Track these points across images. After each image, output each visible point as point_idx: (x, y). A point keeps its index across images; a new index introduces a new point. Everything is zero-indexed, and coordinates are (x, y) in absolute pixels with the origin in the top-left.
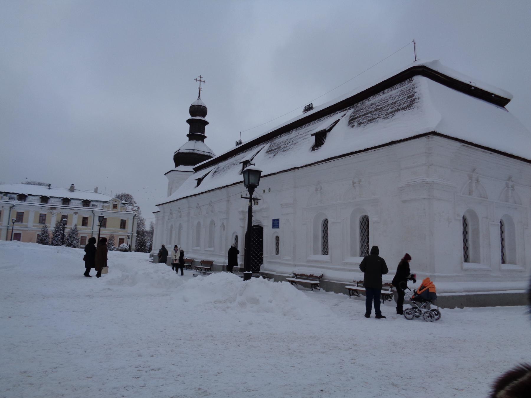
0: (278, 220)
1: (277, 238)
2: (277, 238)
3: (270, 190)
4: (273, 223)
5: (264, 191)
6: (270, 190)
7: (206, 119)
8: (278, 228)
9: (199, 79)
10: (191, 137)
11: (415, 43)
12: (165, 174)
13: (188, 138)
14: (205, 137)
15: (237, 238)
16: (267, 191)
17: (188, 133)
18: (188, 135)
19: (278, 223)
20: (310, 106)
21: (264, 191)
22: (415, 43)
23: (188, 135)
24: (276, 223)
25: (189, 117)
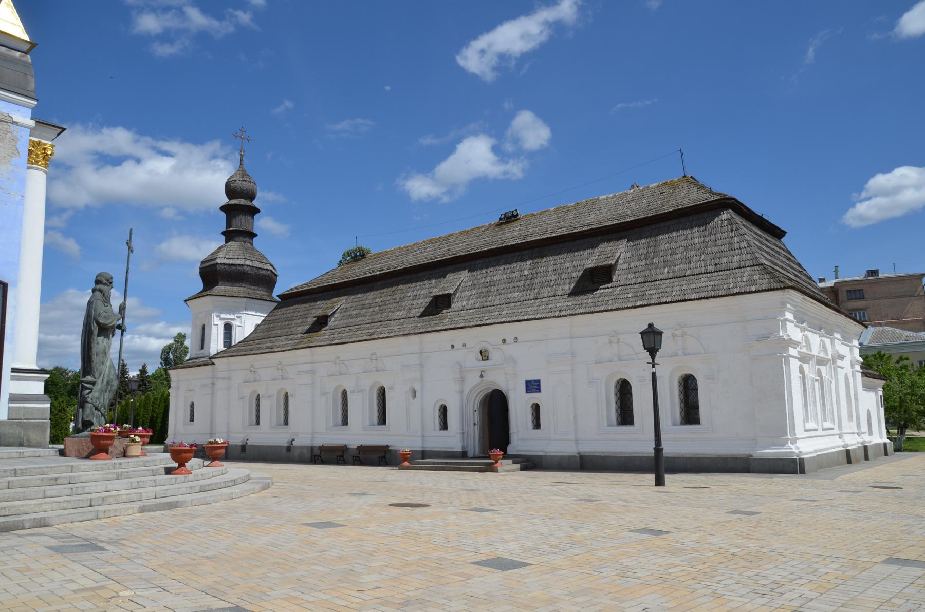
0: (538, 382)
1: (536, 408)
2: (536, 408)
4: (527, 386)
5: (504, 341)
6: (516, 339)
7: (256, 203)
9: (239, 133)
10: (229, 235)
11: (682, 154)
12: (185, 301)
13: (224, 238)
14: (256, 235)
15: (444, 410)
16: (509, 339)
18: (223, 233)
19: (539, 385)
20: (515, 213)
21: (504, 341)
22: (682, 154)
23: (223, 233)
25: (225, 200)
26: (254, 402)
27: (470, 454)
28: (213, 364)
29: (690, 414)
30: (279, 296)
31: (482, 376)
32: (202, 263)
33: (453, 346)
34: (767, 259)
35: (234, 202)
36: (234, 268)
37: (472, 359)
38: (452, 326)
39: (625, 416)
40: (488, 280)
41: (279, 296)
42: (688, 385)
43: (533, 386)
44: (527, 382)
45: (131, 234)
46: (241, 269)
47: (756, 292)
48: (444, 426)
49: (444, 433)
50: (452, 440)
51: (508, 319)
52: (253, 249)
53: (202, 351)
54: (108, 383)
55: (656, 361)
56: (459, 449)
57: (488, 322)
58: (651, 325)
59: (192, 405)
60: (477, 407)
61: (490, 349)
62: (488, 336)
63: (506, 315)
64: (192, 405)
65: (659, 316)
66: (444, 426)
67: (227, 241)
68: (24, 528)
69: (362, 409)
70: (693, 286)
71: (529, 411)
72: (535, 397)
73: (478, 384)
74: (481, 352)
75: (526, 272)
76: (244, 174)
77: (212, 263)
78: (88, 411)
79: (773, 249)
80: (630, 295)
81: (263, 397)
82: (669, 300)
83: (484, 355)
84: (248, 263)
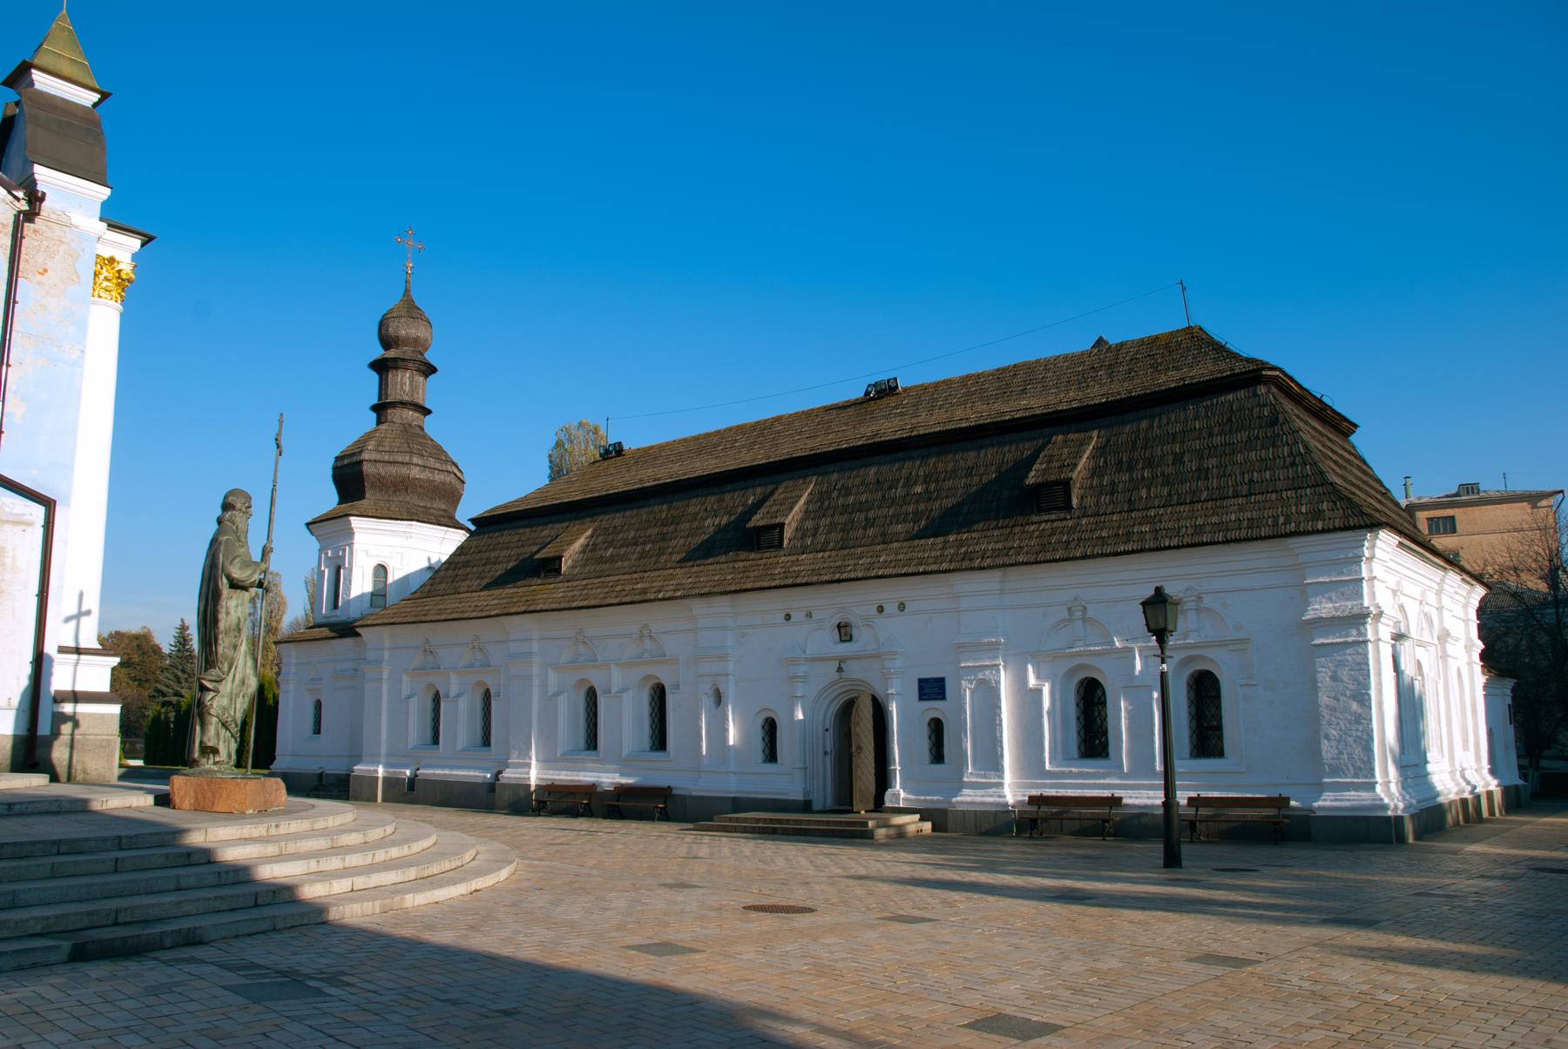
1: (937, 727)
2: (937, 727)
3: (902, 607)
4: (921, 689)
5: (881, 609)
7: (430, 357)
8: (944, 698)
10: (380, 409)
12: (308, 525)
13: (374, 415)
16: (891, 608)
17: (375, 401)
18: (375, 408)
20: (892, 384)
21: (881, 609)
22: (1184, 289)
23: (375, 408)
24: (932, 689)
25: (378, 352)
26: (429, 705)
27: (817, 806)
28: (358, 635)
29: (1207, 738)
30: (473, 521)
31: (840, 669)
32: (337, 459)
33: (788, 617)
34: (1337, 474)
35: (392, 354)
36: (393, 470)
37: (824, 642)
38: (790, 581)
39: (1092, 737)
40: (851, 499)
41: (473, 521)
42: (1205, 688)
43: (932, 689)
44: (921, 681)
45: (281, 422)
46: (404, 470)
47: (1324, 531)
48: (771, 755)
49: (770, 767)
50: (785, 781)
51: (888, 571)
52: (425, 436)
53: (338, 612)
54: (243, 682)
55: (1168, 653)
56: (800, 797)
57: (852, 575)
58: (1158, 590)
59: (318, 706)
60: (829, 723)
61: (853, 620)
62: (856, 601)
63: (886, 564)
64: (318, 706)
65: (1175, 573)
66: (771, 755)
67: (379, 422)
68: (163, 948)
69: (625, 719)
70: (1214, 520)
71: (924, 732)
72: (935, 708)
73: (833, 684)
74: (839, 626)
75: (919, 489)
76: (410, 309)
77: (355, 459)
78: (212, 730)
79: (1341, 457)
80: (1104, 534)
81: (447, 696)
82: (1174, 542)
83: (844, 632)
84: (415, 460)
